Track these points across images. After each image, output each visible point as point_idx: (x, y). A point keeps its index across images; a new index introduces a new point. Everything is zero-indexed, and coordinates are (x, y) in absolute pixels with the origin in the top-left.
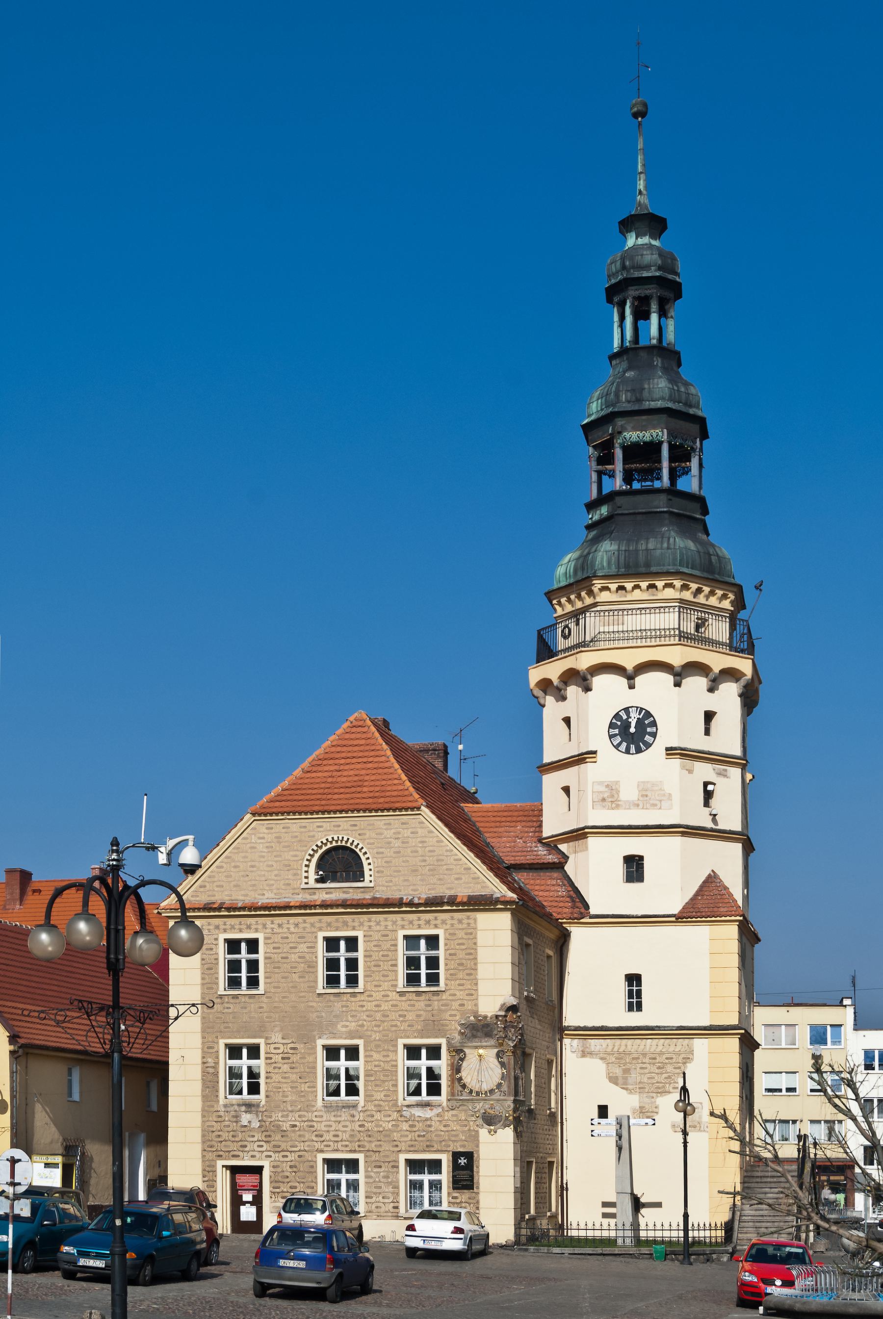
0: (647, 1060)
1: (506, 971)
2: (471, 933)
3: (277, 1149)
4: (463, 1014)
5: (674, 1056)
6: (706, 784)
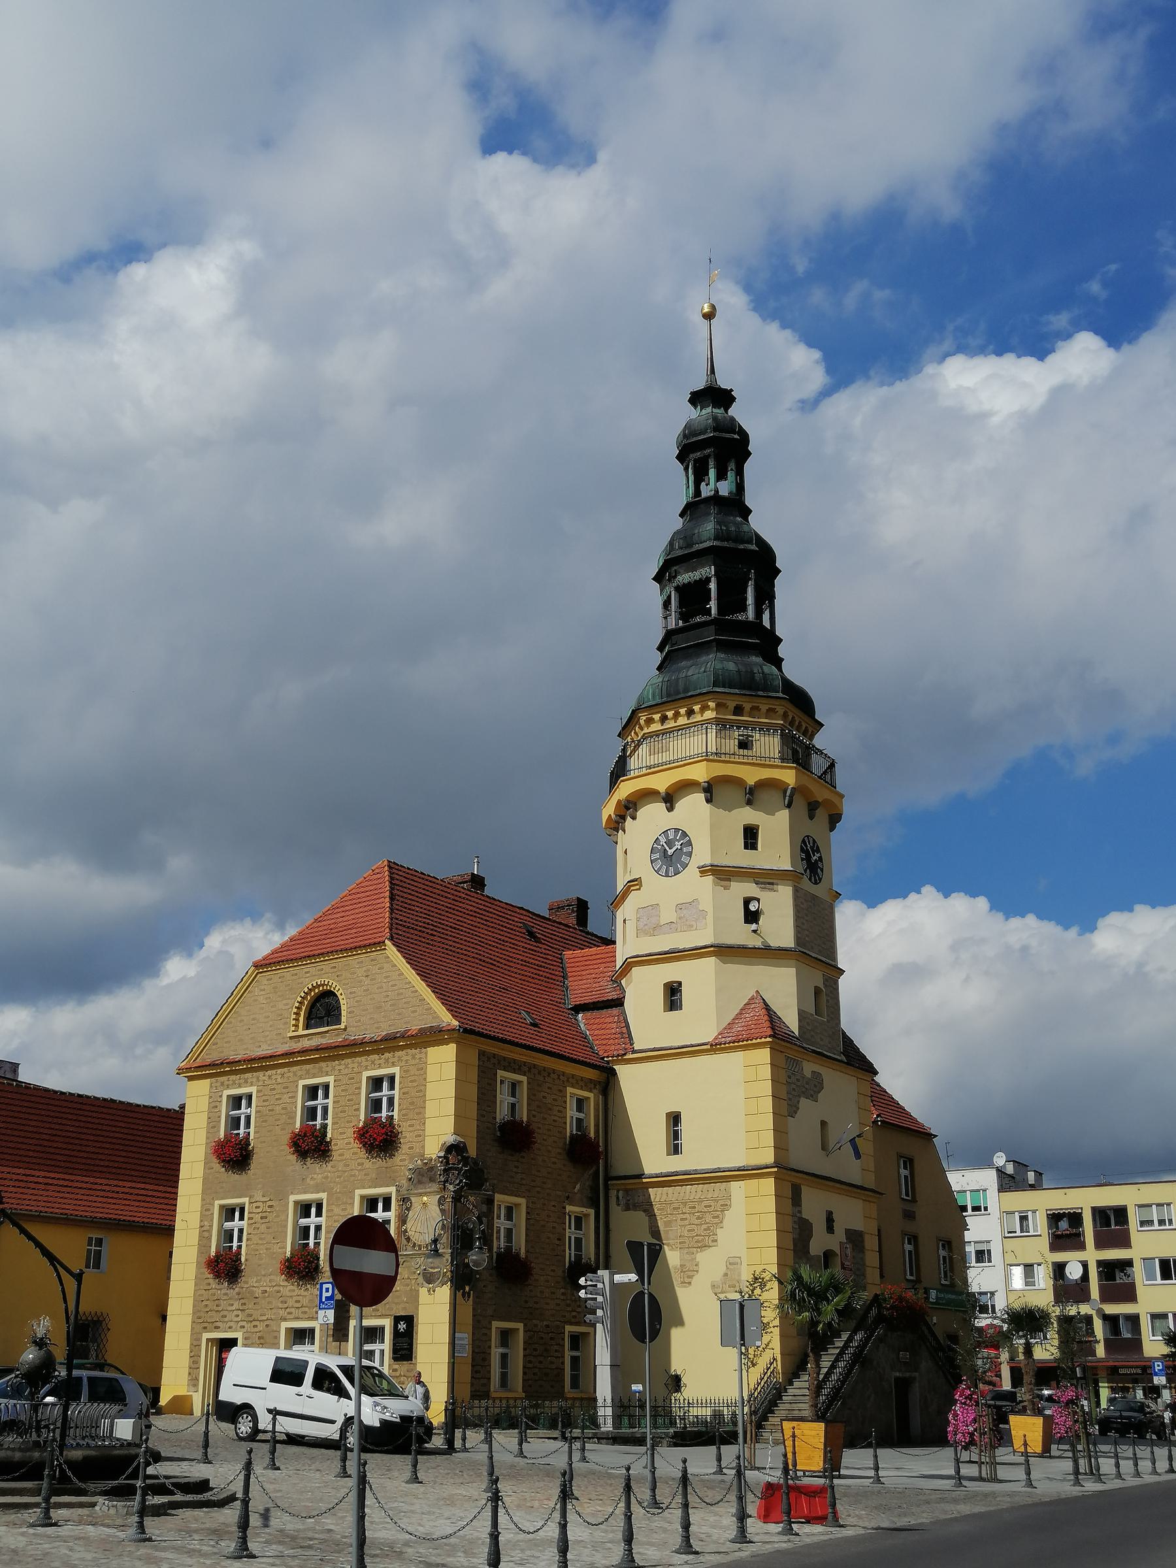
0: (687, 1210)
1: (450, 1107)
2: (422, 1069)
3: (251, 1319)
4: (411, 1158)
6: (747, 902)
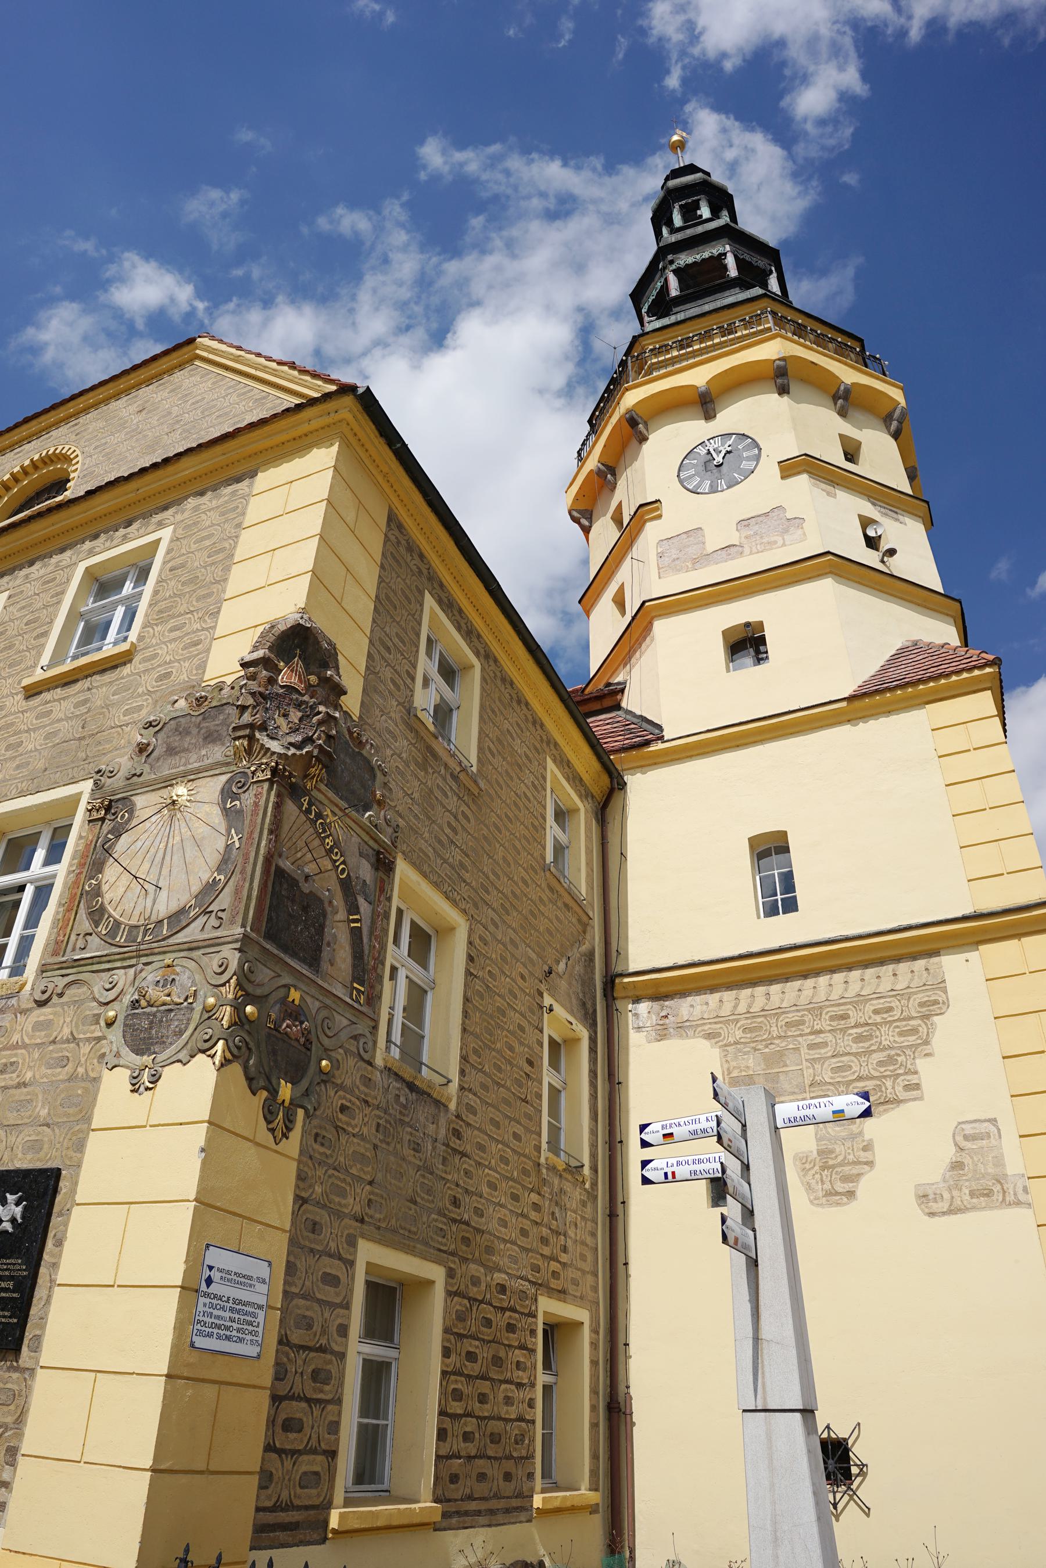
0: (825, 1024)
5: (895, 1004)
6: (866, 522)
